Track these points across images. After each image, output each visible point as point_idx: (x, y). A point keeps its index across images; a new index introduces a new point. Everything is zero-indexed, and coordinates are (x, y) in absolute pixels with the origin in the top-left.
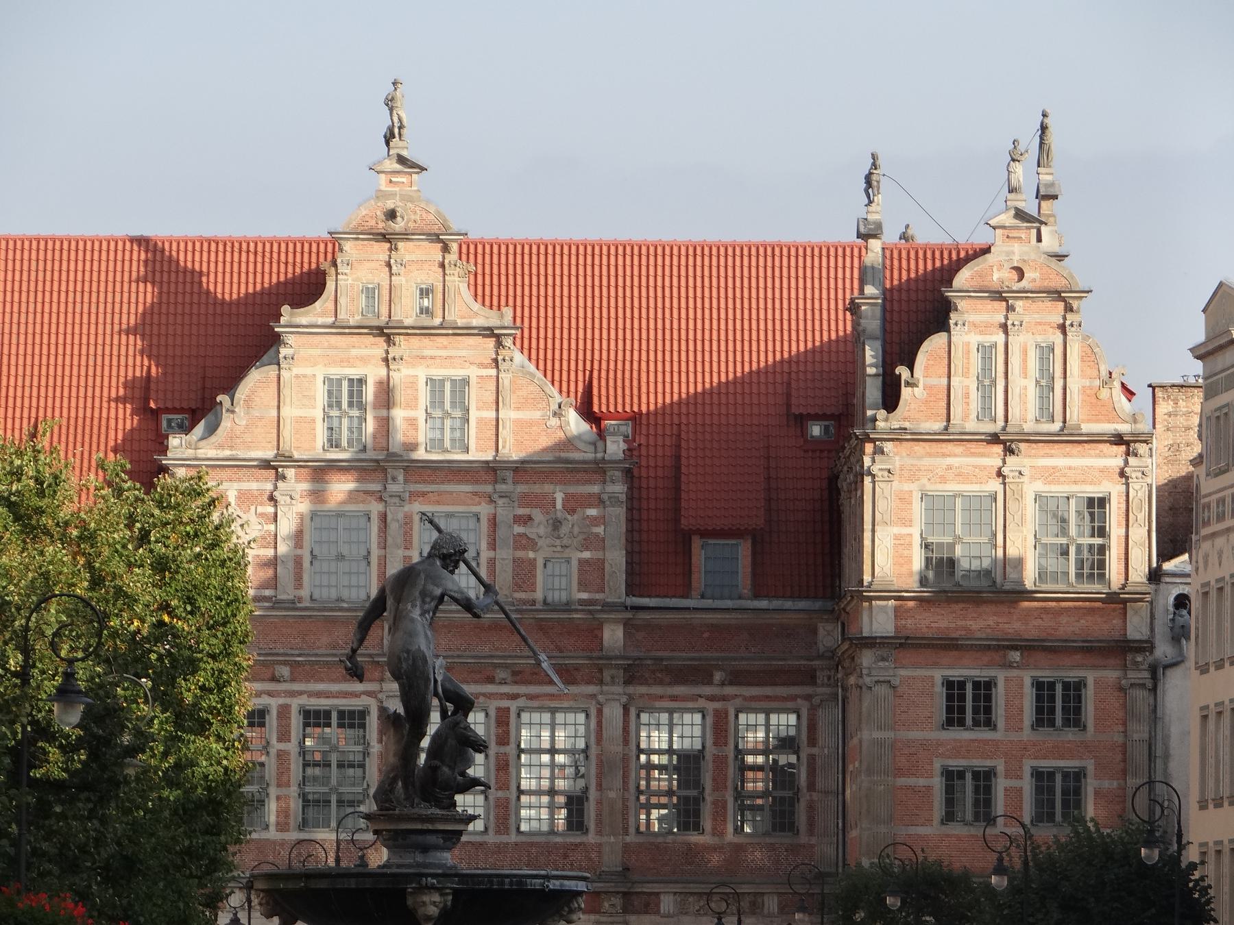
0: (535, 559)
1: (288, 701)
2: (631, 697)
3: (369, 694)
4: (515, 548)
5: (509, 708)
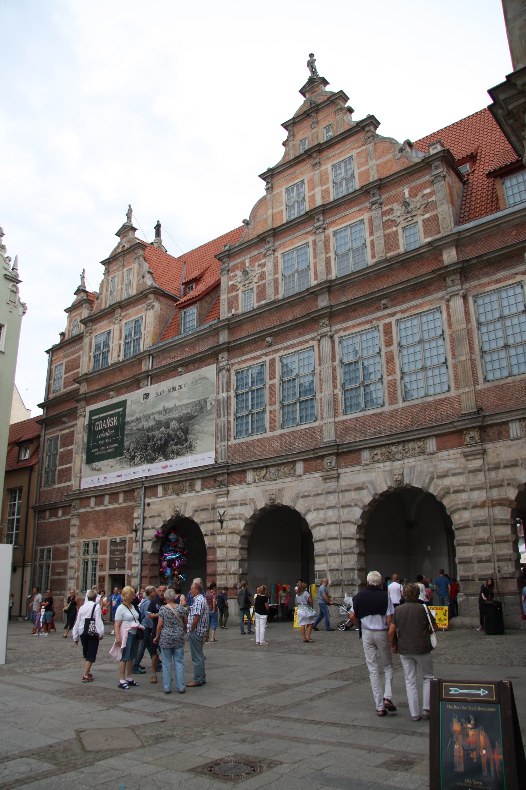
0: (397, 231)
2: (468, 290)
4: (384, 230)
5: (391, 323)
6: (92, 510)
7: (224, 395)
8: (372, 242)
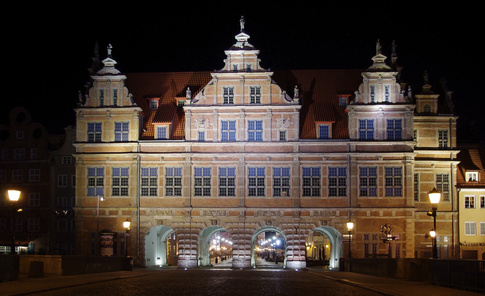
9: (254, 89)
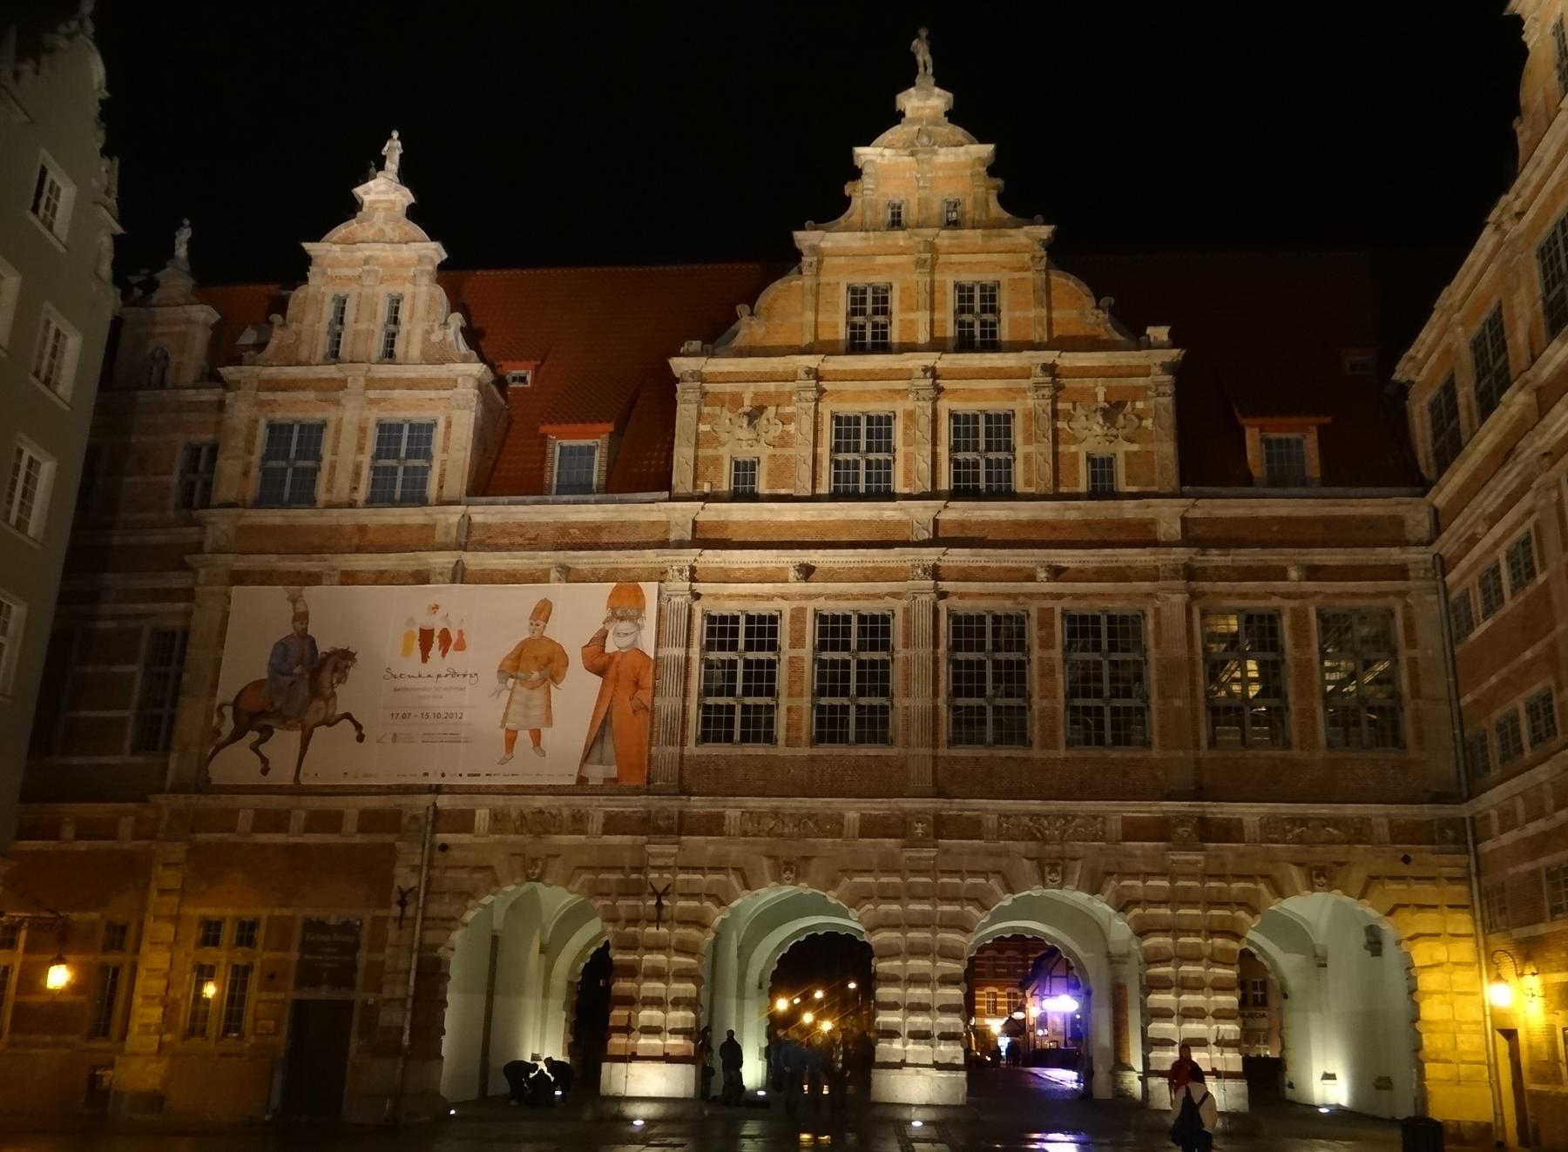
1: (803, 603)
3: (894, 595)
5: (1053, 608)
6: (240, 840)
7: (679, 652)
8: (1027, 457)
9: (971, 290)
